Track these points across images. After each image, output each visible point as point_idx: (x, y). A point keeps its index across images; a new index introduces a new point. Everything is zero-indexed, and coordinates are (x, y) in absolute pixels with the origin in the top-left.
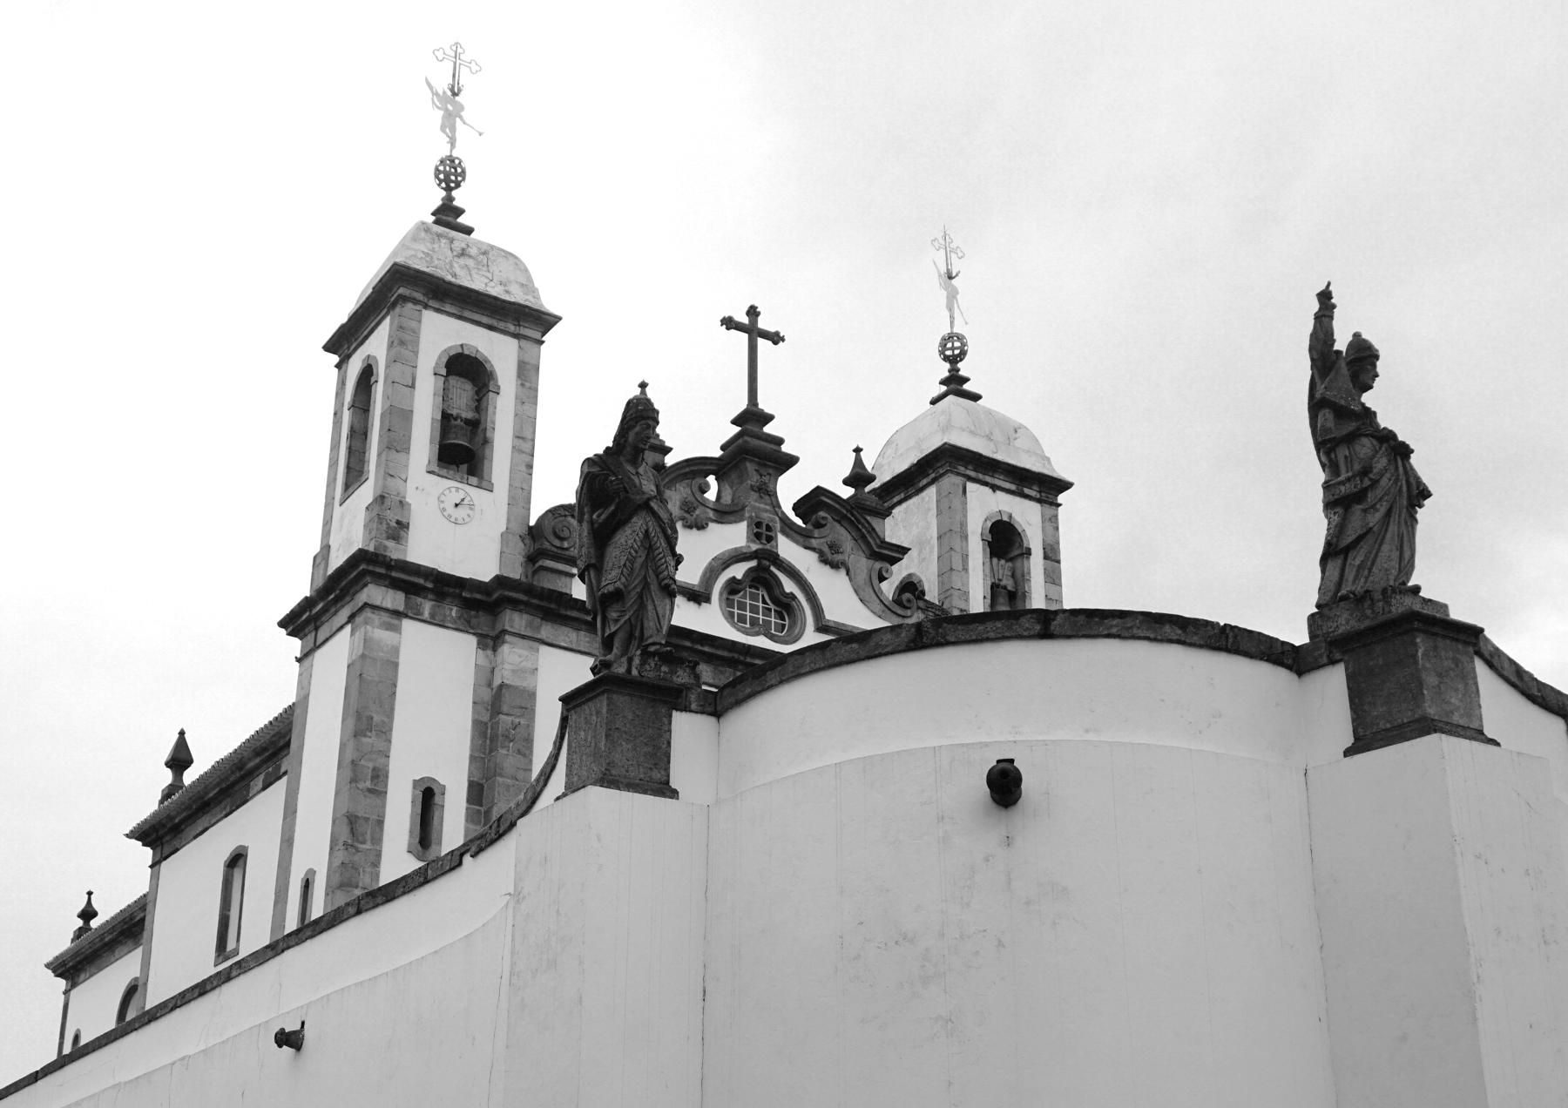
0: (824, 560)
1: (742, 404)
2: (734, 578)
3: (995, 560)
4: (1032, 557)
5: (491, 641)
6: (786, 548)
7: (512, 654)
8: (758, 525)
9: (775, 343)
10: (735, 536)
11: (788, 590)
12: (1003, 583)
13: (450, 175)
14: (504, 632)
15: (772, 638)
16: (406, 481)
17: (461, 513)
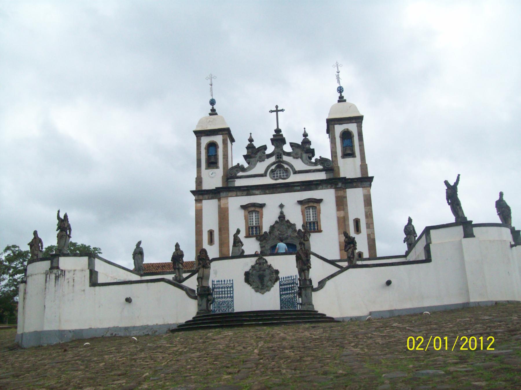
0: (294, 158)
1: (276, 128)
2: (272, 170)
3: (346, 140)
4: (354, 138)
5: (219, 200)
6: (285, 158)
7: (223, 201)
8: (278, 155)
9: (283, 111)
10: (273, 159)
12: (348, 145)
13: (212, 102)
14: (221, 197)
17: (213, 175)
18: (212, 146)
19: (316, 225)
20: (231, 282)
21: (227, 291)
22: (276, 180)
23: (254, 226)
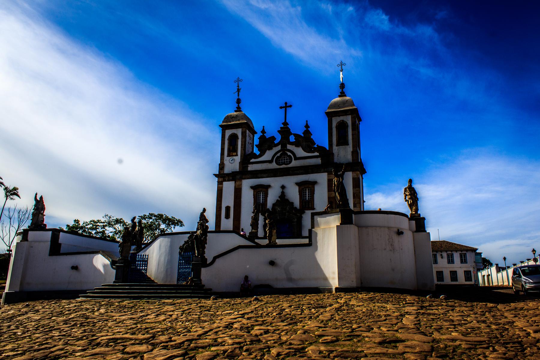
2: (278, 156)
6: (289, 147)
10: (279, 148)
11: (289, 154)
15: (286, 164)
16: (224, 160)
17: (233, 161)
18: (233, 138)
19: (310, 204)
20: (147, 257)
21: (143, 264)
22: (280, 165)
23: (261, 204)
